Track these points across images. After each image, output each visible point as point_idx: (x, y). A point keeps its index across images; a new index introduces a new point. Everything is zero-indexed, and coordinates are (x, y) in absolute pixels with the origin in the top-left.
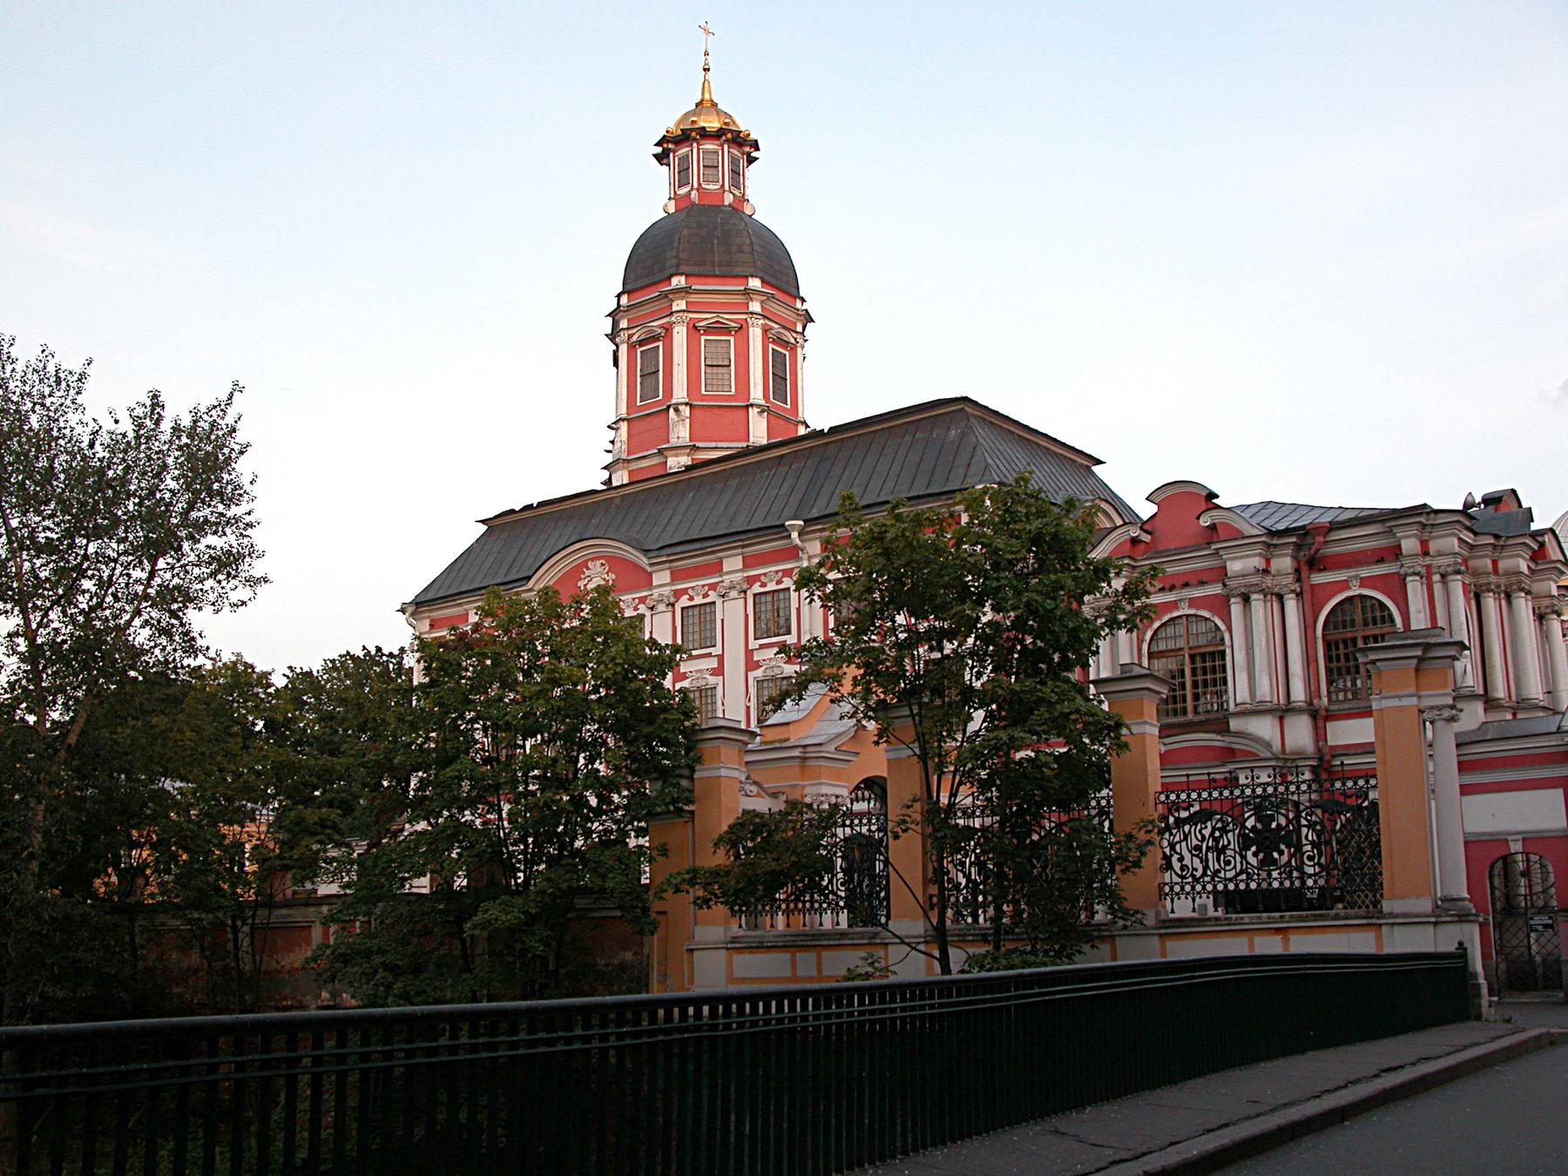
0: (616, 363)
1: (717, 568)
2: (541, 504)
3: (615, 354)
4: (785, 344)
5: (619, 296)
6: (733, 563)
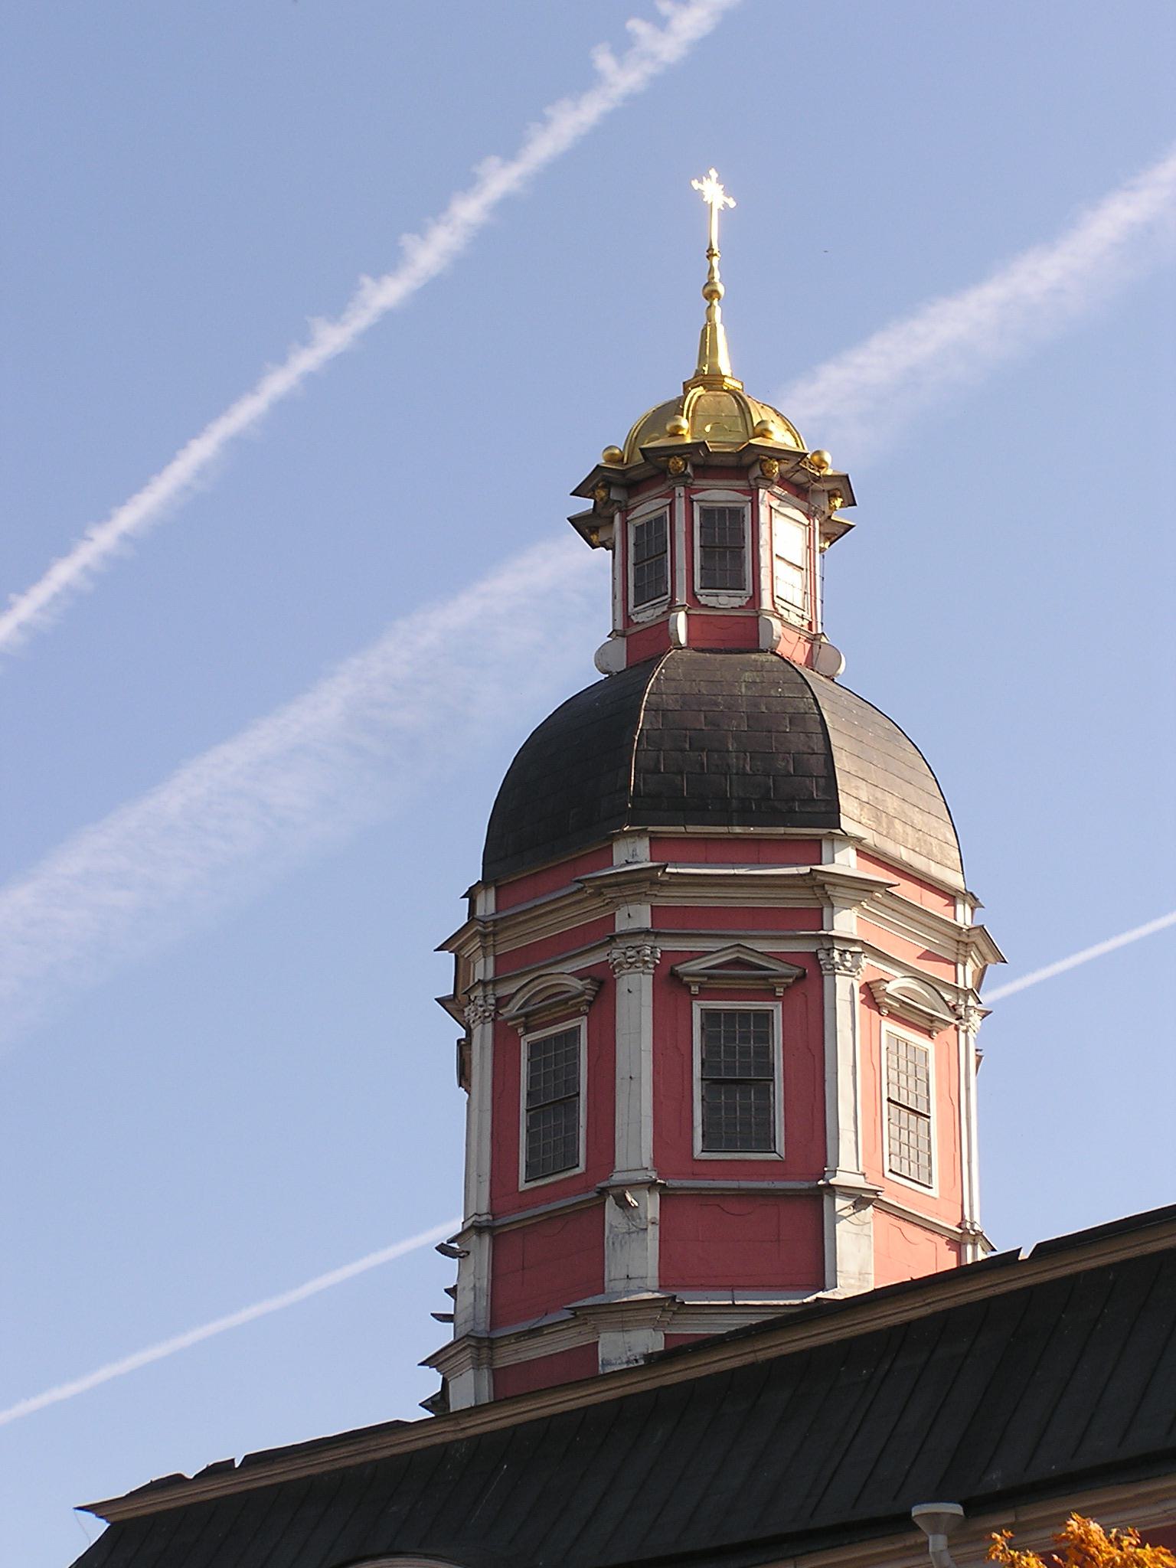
2: (252, 1461)
3: (464, 1047)
4: (928, 1026)
5: (471, 894)
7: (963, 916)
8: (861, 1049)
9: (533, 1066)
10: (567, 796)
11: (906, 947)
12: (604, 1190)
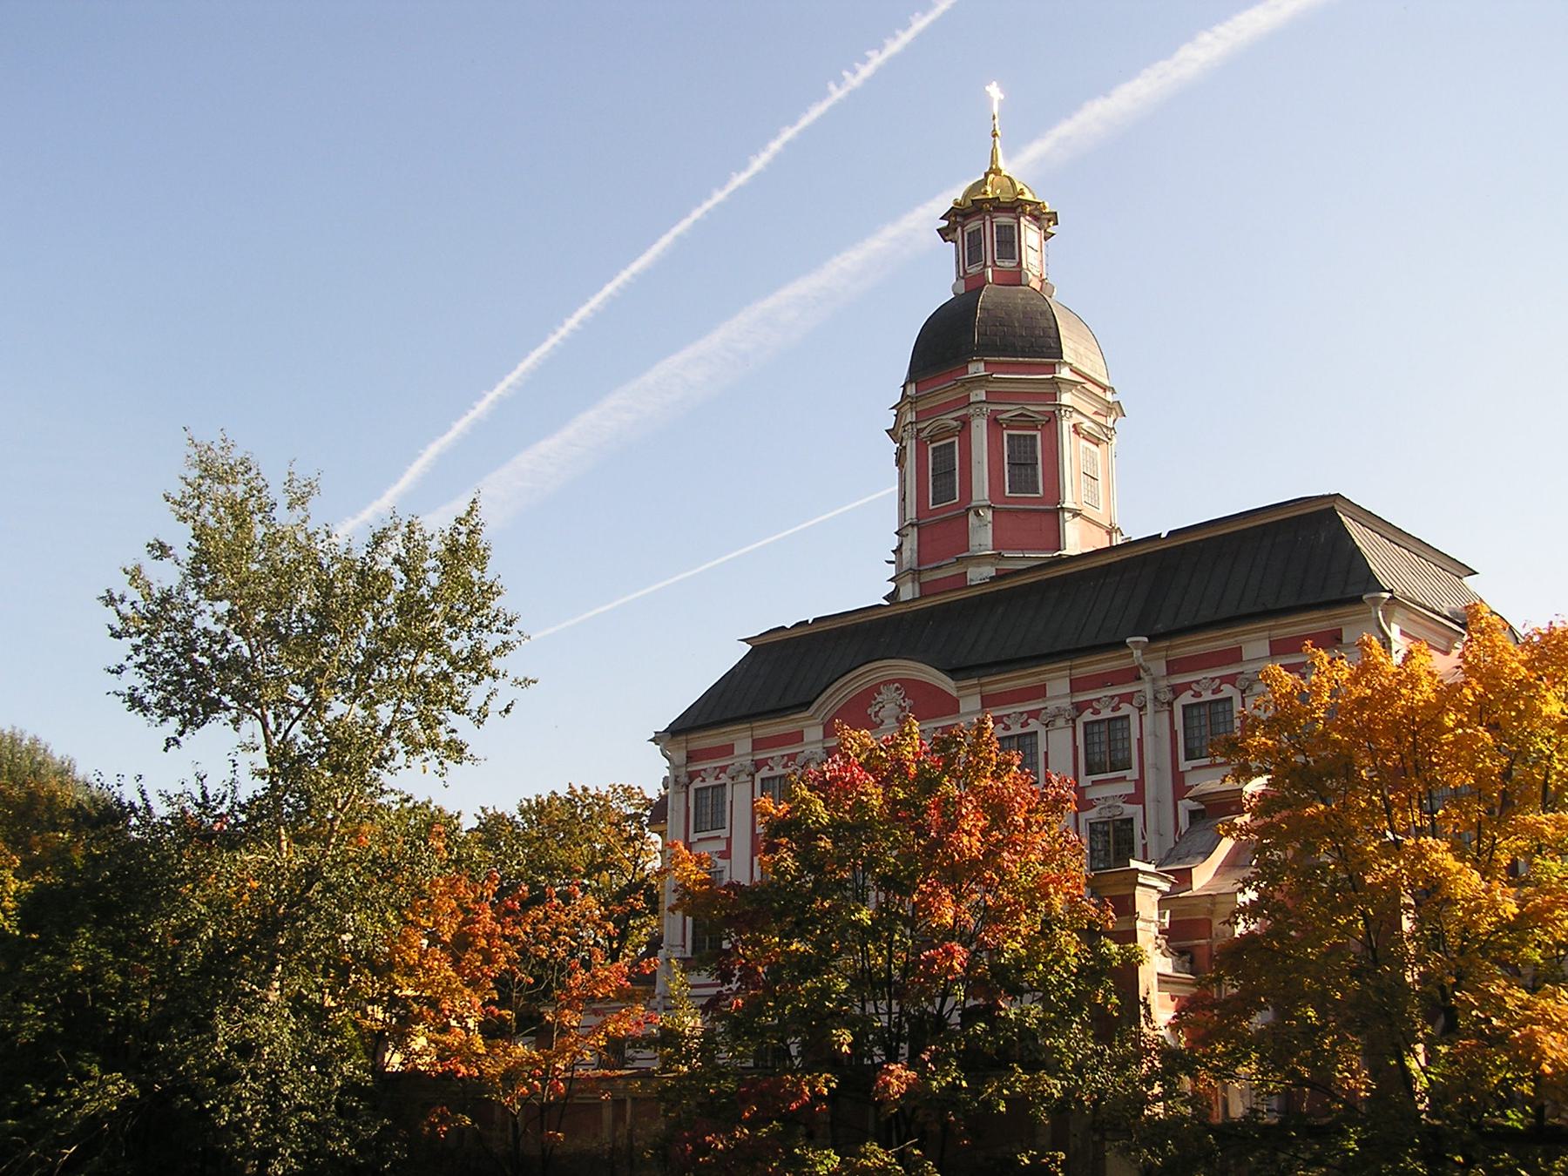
0: (900, 461)
1: (1039, 692)
4: (1097, 442)
6: (1058, 687)
7: (1109, 397)
8: (1073, 451)
9: (934, 458)
10: (945, 346)
11: (1088, 409)
12: (967, 509)
